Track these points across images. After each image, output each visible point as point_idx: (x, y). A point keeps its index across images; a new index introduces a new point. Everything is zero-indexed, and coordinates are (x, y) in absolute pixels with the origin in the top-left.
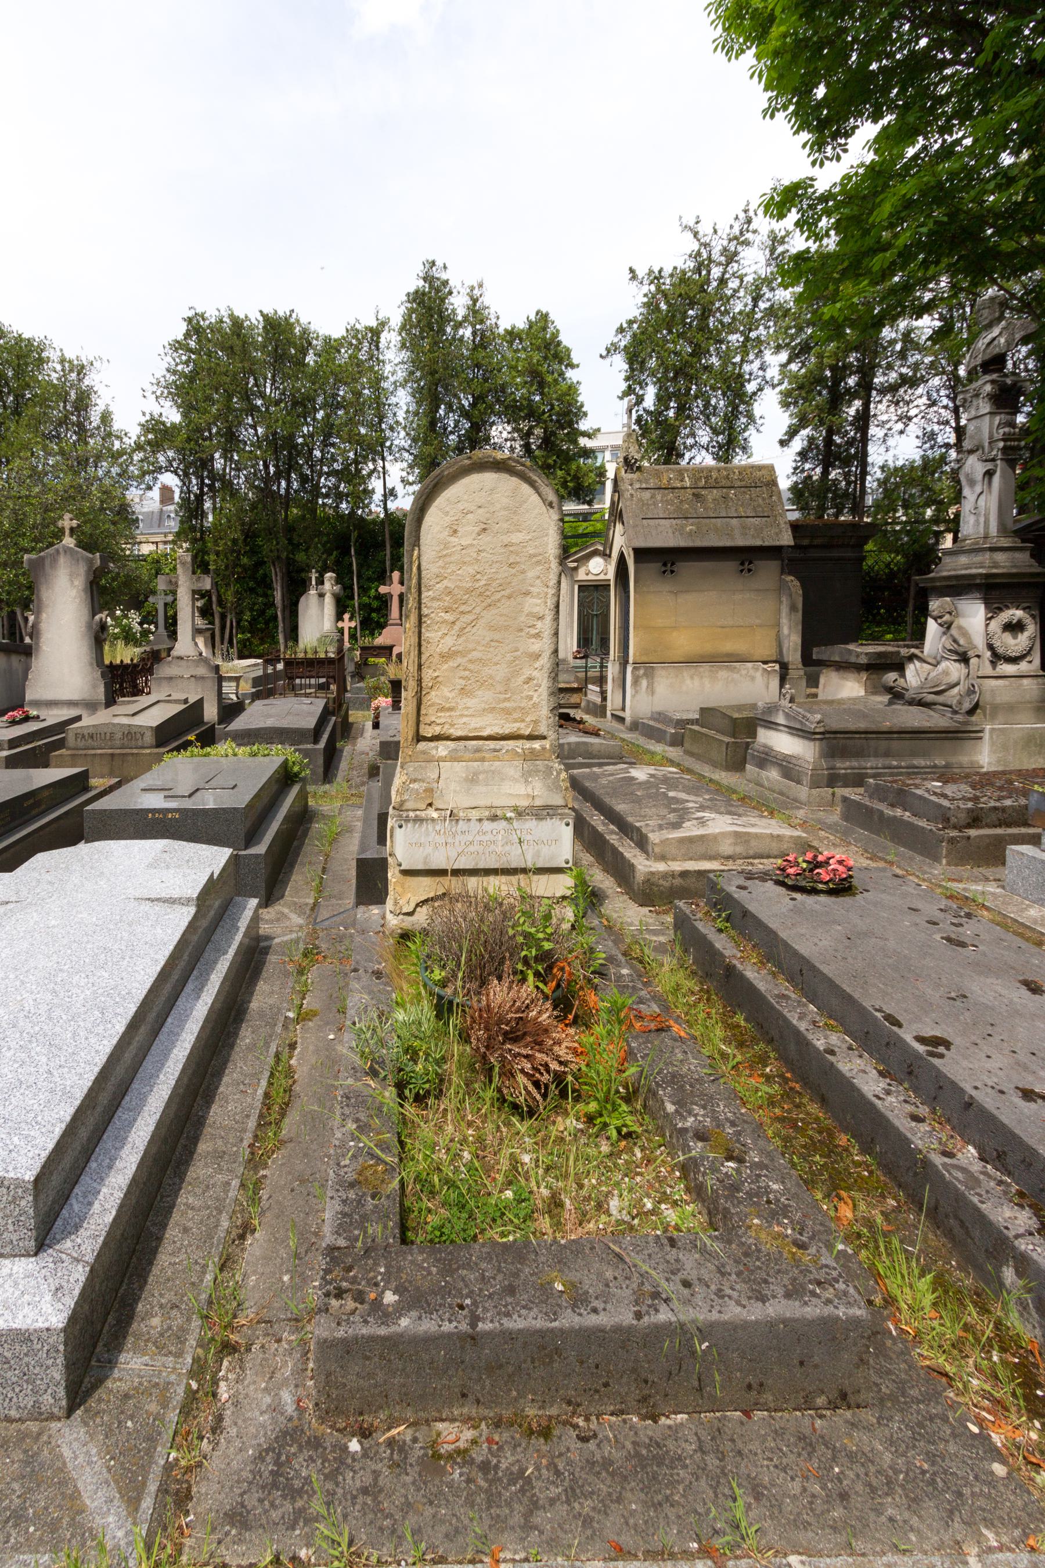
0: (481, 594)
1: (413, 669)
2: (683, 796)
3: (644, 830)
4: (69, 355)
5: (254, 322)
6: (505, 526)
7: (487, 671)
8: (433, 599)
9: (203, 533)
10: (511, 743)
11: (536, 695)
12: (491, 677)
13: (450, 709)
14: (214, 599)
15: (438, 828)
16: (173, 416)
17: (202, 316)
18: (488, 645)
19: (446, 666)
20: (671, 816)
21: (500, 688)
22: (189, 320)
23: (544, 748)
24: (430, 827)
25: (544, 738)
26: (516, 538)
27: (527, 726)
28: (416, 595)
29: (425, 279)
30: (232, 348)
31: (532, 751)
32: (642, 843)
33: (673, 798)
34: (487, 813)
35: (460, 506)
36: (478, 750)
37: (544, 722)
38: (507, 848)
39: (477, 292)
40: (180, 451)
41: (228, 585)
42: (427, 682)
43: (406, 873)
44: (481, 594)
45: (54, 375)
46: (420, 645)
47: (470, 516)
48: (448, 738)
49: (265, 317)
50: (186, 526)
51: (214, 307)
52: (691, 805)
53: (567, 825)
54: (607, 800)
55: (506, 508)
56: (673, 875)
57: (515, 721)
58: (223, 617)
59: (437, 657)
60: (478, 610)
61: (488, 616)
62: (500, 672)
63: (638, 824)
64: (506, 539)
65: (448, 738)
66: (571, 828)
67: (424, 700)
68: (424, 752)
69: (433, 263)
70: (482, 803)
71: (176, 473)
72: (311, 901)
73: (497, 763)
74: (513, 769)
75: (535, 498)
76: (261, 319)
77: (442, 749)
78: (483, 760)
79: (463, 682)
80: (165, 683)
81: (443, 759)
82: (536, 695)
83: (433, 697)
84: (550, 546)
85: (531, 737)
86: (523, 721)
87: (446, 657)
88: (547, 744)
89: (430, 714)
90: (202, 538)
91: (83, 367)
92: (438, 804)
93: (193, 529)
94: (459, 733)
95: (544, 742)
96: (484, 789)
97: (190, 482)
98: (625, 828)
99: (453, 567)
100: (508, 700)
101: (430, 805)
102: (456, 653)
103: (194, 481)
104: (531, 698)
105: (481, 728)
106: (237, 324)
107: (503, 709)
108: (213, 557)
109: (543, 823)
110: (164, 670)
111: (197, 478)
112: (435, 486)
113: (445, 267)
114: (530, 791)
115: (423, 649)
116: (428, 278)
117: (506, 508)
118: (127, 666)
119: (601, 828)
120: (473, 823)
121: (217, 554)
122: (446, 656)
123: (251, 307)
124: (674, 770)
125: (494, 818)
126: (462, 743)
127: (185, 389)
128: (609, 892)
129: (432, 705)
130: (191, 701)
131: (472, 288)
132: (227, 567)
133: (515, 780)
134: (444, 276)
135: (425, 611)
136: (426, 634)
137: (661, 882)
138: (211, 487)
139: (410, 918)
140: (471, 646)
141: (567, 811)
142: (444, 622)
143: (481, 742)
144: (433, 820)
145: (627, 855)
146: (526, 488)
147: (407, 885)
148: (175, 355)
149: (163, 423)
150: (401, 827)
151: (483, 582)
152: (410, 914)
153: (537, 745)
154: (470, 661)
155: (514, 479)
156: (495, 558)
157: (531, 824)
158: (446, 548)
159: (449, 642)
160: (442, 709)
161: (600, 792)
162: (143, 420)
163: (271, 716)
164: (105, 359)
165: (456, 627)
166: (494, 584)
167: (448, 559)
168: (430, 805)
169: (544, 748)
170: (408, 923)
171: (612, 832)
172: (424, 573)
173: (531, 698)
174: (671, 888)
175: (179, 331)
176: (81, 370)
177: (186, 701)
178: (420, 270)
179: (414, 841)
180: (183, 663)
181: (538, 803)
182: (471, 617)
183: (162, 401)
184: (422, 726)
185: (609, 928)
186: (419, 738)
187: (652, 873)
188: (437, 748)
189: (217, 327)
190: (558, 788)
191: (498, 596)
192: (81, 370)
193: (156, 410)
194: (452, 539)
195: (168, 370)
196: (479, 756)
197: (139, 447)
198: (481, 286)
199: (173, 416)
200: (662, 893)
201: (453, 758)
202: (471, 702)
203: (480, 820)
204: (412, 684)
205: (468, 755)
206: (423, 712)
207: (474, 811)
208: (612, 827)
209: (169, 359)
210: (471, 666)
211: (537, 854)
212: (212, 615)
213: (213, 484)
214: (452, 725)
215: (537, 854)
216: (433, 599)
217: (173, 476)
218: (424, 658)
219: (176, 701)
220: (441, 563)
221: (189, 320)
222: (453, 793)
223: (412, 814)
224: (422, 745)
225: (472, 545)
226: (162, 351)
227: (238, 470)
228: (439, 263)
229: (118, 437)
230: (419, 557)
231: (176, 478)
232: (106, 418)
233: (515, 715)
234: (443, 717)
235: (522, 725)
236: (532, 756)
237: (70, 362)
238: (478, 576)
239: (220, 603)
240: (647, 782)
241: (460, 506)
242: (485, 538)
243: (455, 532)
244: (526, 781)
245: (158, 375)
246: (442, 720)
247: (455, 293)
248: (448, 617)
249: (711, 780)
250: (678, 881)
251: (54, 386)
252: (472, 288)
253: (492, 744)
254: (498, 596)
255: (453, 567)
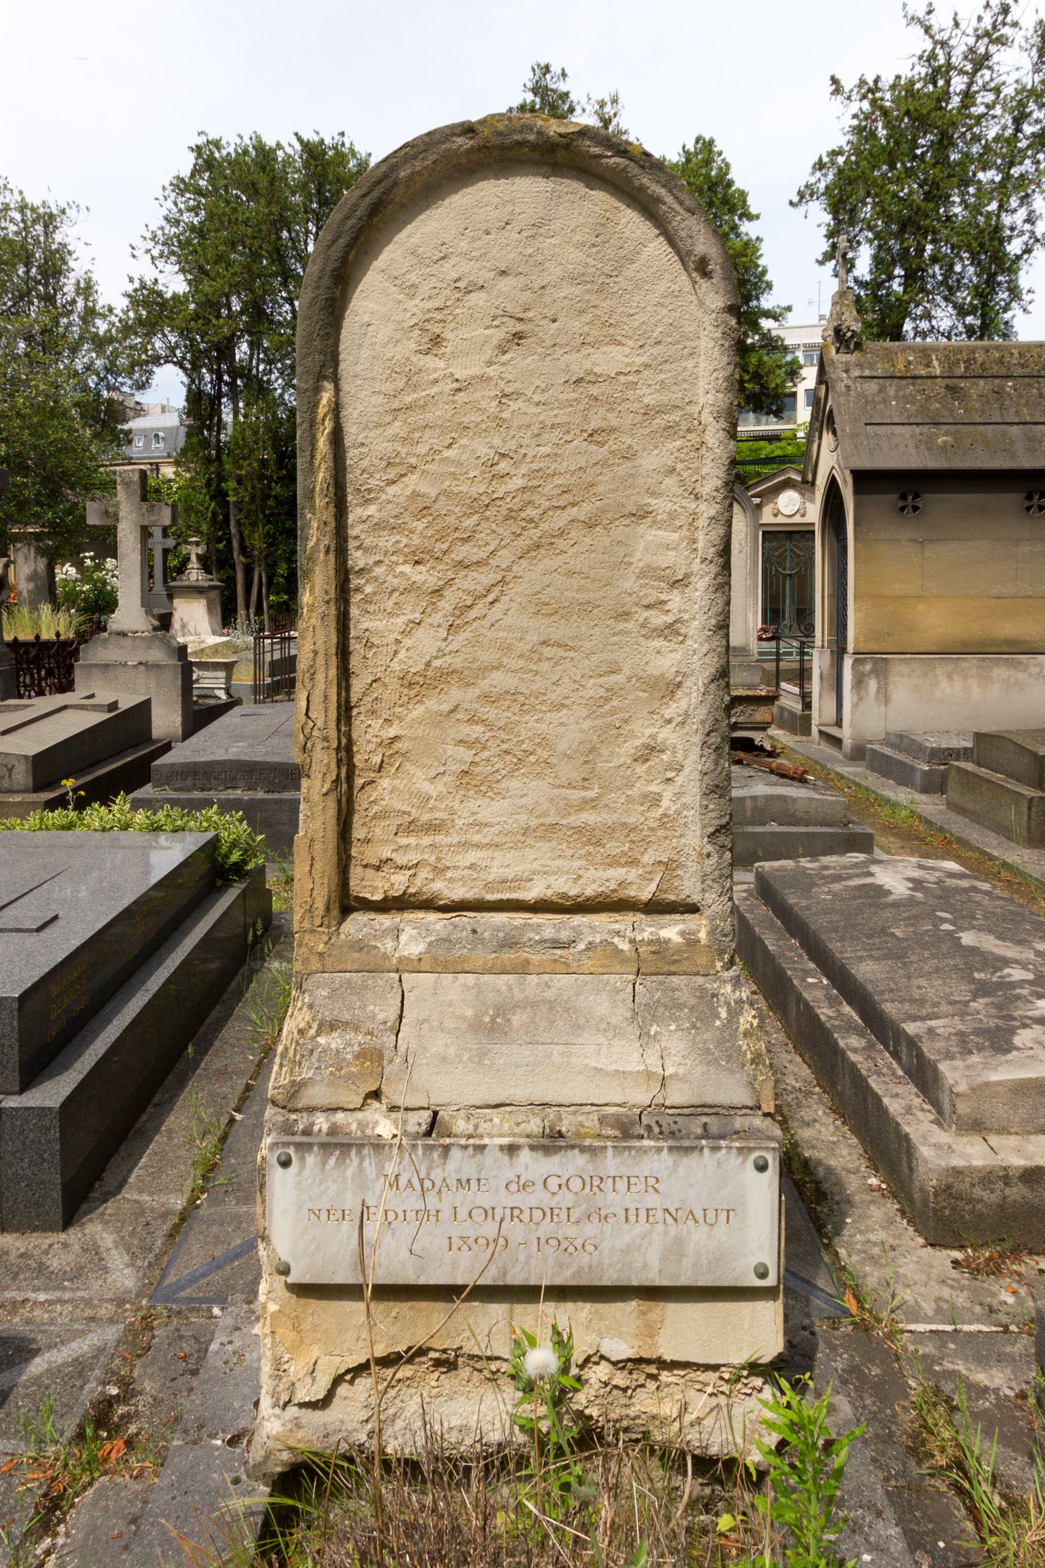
0: (511, 516)
1: (325, 716)
2: (990, 944)
3: (927, 1049)
4: (34, 199)
5: (289, 151)
6: (576, 325)
7: (532, 725)
8: (379, 526)
9: (219, 450)
10: (600, 920)
11: (668, 792)
12: (544, 742)
13: (434, 828)
14: (235, 544)
15: (391, 1168)
16: (174, 283)
17: (217, 144)
18: (534, 655)
19: (418, 711)
20: (979, 1004)
21: (569, 772)
22: (198, 150)
23: (691, 943)
24: (370, 1166)
25: (693, 909)
26: (609, 359)
27: (646, 878)
28: (329, 515)
29: (535, 91)
30: (253, 184)
31: (660, 947)
32: (924, 1077)
33: (974, 950)
34: (534, 1125)
35: (449, 270)
36: (509, 943)
37: (693, 867)
38: (590, 1229)
39: (608, 109)
40: (184, 332)
41: (254, 524)
42: (366, 754)
43: (305, 1290)
44: (511, 516)
45: (13, 228)
46: (343, 653)
47: (477, 298)
48: (428, 905)
49: (306, 146)
50: (195, 440)
51: (233, 135)
52: (1016, 974)
53: (762, 1168)
54: (835, 946)
55: (577, 279)
56: (1005, 1176)
57: (613, 862)
58: (248, 571)
59: (393, 684)
60: (504, 558)
61: (532, 574)
62: (570, 729)
63: (911, 1028)
64: (578, 364)
65: (428, 905)
66: (771, 1179)
67: (361, 801)
68: (360, 946)
69: (547, 69)
70: (520, 1093)
71: (180, 364)
72: (179, 1203)
73: (563, 980)
74: (605, 999)
75: (657, 248)
76: (298, 147)
77: (411, 936)
78: (522, 969)
79: (468, 755)
80: (96, 674)
81: (415, 966)
82: (668, 792)
83: (384, 795)
84: (703, 384)
85: (656, 907)
86: (634, 862)
87: (419, 684)
88: (700, 927)
89: (375, 838)
90: (219, 457)
91: (51, 216)
92: (395, 1093)
93: (205, 444)
94: (459, 893)
95: (692, 921)
96: (524, 1054)
97: (201, 378)
98: (879, 1026)
99: (430, 440)
100: (586, 804)
101: (376, 1095)
102: (446, 675)
103: (207, 377)
104: (655, 800)
105: (520, 881)
106: (265, 155)
107: (578, 830)
108: (232, 484)
109: (692, 1161)
110: (95, 653)
111: (211, 371)
112: (376, 208)
113: (564, 74)
114: (653, 1062)
115: (354, 662)
116: (538, 89)
117: (577, 279)
118: (48, 644)
119: (824, 1012)
120: (491, 1157)
121: (240, 481)
122: (419, 684)
123: (283, 131)
124: (952, 866)
125: (552, 1141)
126: (467, 919)
127: (192, 248)
128: (852, 1184)
129: (383, 815)
130: (123, 706)
131: (602, 104)
132: (253, 498)
133: (613, 1031)
134: (562, 87)
135: (357, 559)
136: (361, 623)
137: (978, 1192)
138: (232, 385)
139: (318, 1417)
140: (486, 657)
141: (758, 1122)
142: (412, 588)
143: (519, 918)
144: (378, 1146)
145: (893, 1106)
146: (631, 223)
147: (307, 1324)
148: (180, 199)
149: (160, 294)
150: (286, 1164)
151: (518, 482)
152: (323, 1403)
153: (672, 930)
154: (486, 698)
155: (599, 196)
156: (548, 416)
157: (656, 1162)
158: (411, 385)
159: (426, 643)
160: (411, 827)
161: (818, 923)
162: (130, 288)
163: (242, 737)
164: (83, 207)
165: (446, 605)
166: (548, 488)
167: (417, 417)
168: (376, 1095)
169: (691, 943)
170: (313, 1433)
171: (850, 1028)
172: (352, 455)
173: (655, 800)
174: (1002, 1207)
175: (185, 164)
176: (49, 221)
177: (113, 706)
178: (527, 77)
179: (324, 1204)
180: (127, 642)
181: (677, 1095)
182: (485, 578)
183: (160, 264)
184: (356, 873)
185: (864, 1328)
186: (346, 904)
187: (957, 1172)
188: (397, 933)
189: (236, 162)
190: (732, 1054)
191: (559, 520)
192: (49, 221)
193: (149, 274)
194: (429, 362)
195: (166, 219)
196: (510, 958)
197: (127, 329)
198: (615, 101)
199: (174, 283)
200: (981, 1216)
201: (441, 962)
202: (491, 810)
203: (512, 1149)
204: (322, 764)
205: (483, 956)
206: (358, 832)
207: (496, 1116)
208: (847, 1009)
209: (169, 204)
210: (489, 712)
211: (677, 1248)
212: (233, 567)
213: (234, 381)
214: (439, 871)
215: (677, 1248)
216: (379, 526)
217: (176, 370)
218: (357, 686)
219: (95, 708)
220: (397, 427)
221: (198, 150)
222: (442, 1073)
223: (321, 1122)
224: (357, 924)
225: (483, 379)
226: (160, 194)
227: (270, 362)
228: (556, 69)
229: (104, 317)
230: (336, 409)
231: (180, 372)
232: (86, 289)
233: (613, 847)
234: (414, 848)
235: (633, 874)
236: (657, 961)
237: (33, 210)
238: (504, 466)
239: (243, 549)
240: (910, 901)
241: (449, 270)
242: (520, 360)
243: (437, 341)
244: (643, 1035)
245: (153, 227)
246: (412, 857)
247: (578, 111)
248: (424, 576)
249: (1005, 865)
250: (1017, 1192)
251: (11, 242)
252: (602, 104)
253: (548, 924)
254: (559, 520)
255: (430, 440)
